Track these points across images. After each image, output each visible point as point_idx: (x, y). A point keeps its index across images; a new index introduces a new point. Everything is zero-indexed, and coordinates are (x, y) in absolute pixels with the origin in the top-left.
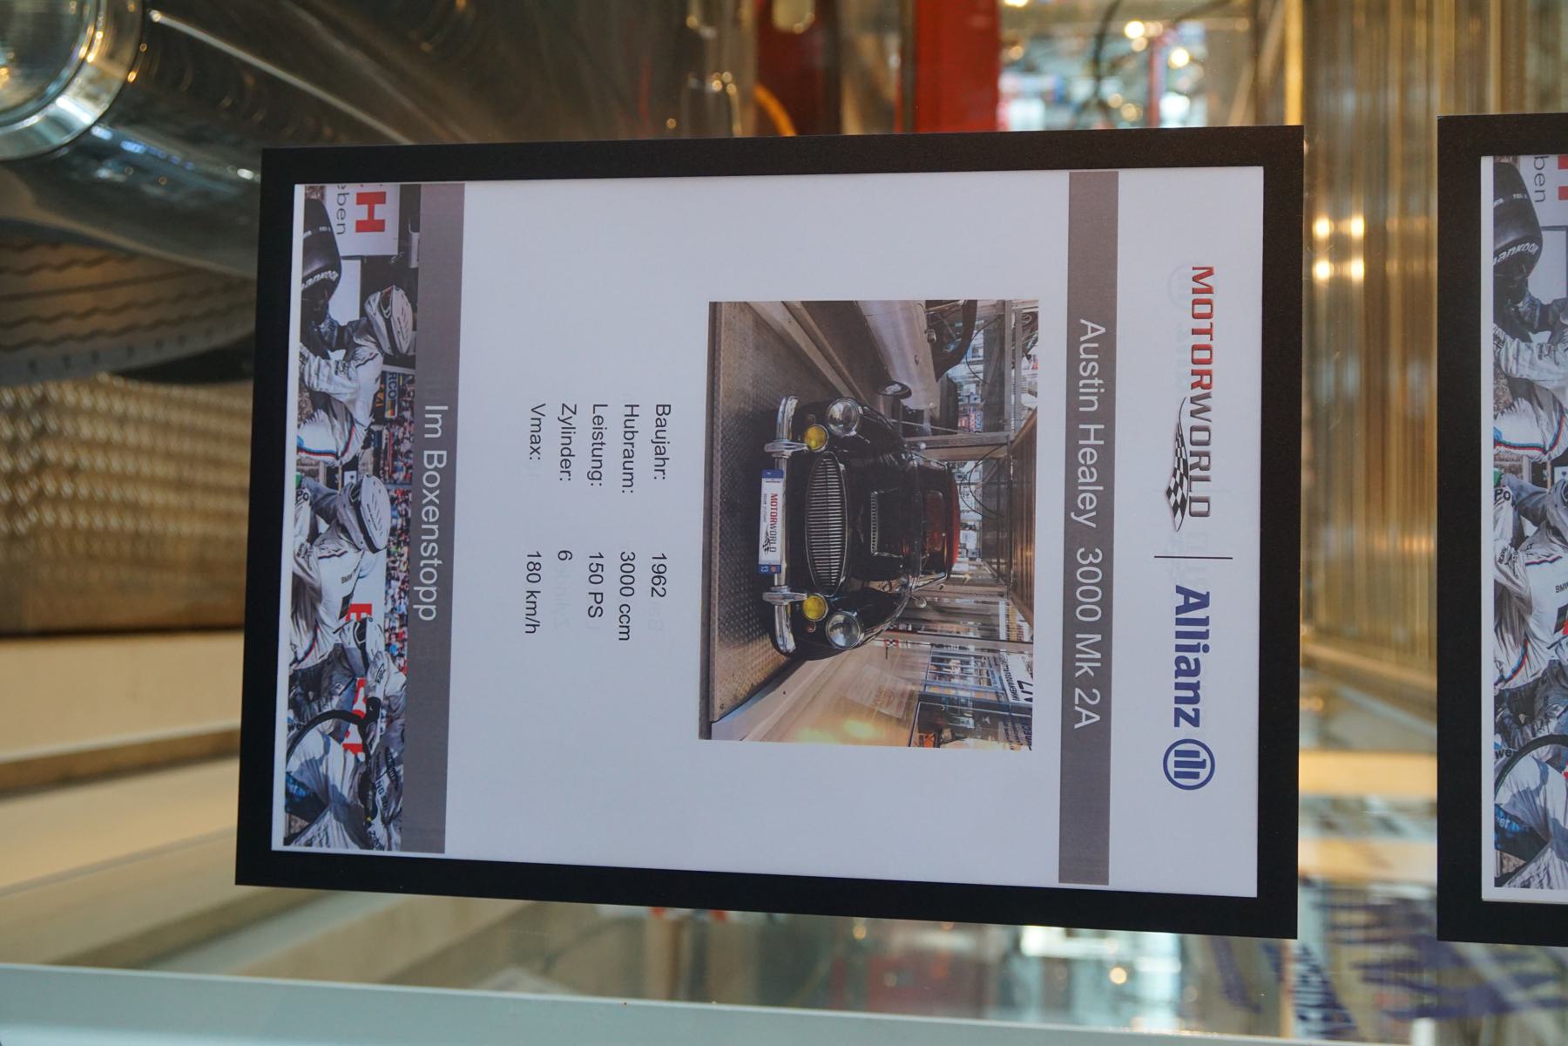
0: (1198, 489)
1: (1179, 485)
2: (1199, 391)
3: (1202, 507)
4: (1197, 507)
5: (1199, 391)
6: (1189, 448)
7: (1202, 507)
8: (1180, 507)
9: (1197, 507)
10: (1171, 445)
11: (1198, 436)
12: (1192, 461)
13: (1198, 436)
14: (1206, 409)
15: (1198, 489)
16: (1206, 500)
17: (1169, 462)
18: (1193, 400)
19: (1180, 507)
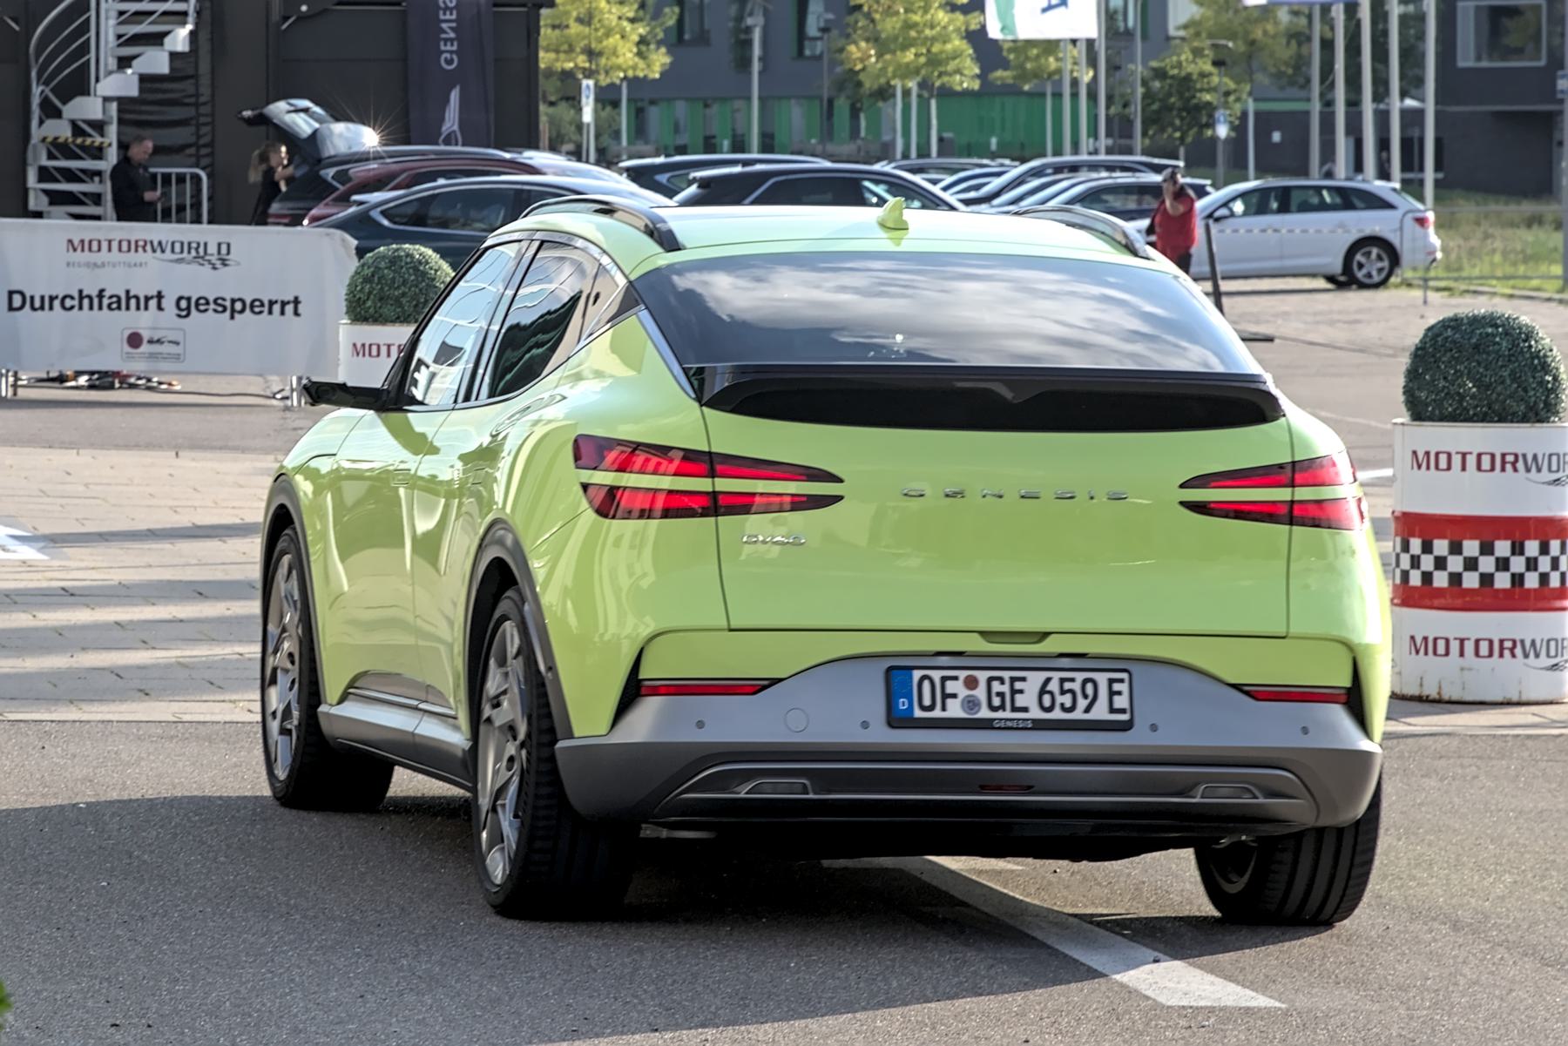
0: (212, 249)
1: (209, 262)
2: (148, 248)
3: (224, 248)
4: (224, 249)
5: (148, 248)
6: (185, 255)
7: (224, 248)
8: (224, 263)
9: (224, 249)
10: (183, 266)
11: (177, 247)
12: (193, 253)
13: (177, 247)
14: (160, 243)
15: (212, 249)
16: (219, 245)
17: (195, 267)
18: (154, 251)
19: (224, 263)
